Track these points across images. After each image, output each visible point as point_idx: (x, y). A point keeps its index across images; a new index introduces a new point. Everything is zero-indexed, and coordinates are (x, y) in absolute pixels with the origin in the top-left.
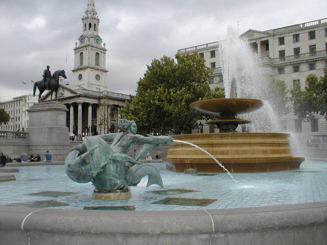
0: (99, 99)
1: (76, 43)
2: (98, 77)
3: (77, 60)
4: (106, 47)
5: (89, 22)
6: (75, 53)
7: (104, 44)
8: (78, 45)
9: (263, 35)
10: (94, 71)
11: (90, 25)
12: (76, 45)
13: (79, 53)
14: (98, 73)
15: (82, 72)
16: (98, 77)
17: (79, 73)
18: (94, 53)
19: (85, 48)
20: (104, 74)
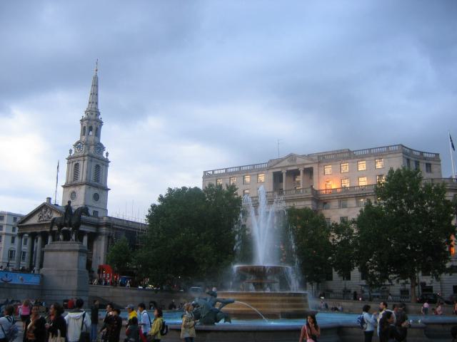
0: (98, 226)
1: (71, 151)
2: (96, 197)
3: (70, 172)
4: (110, 158)
5: (89, 125)
6: (69, 163)
7: (107, 154)
8: (73, 153)
9: (307, 161)
10: (92, 189)
11: (91, 129)
12: (70, 153)
13: (74, 163)
14: (97, 191)
15: (77, 189)
16: (96, 197)
17: (72, 189)
18: (93, 165)
19: (82, 158)
20: (105, 192)
